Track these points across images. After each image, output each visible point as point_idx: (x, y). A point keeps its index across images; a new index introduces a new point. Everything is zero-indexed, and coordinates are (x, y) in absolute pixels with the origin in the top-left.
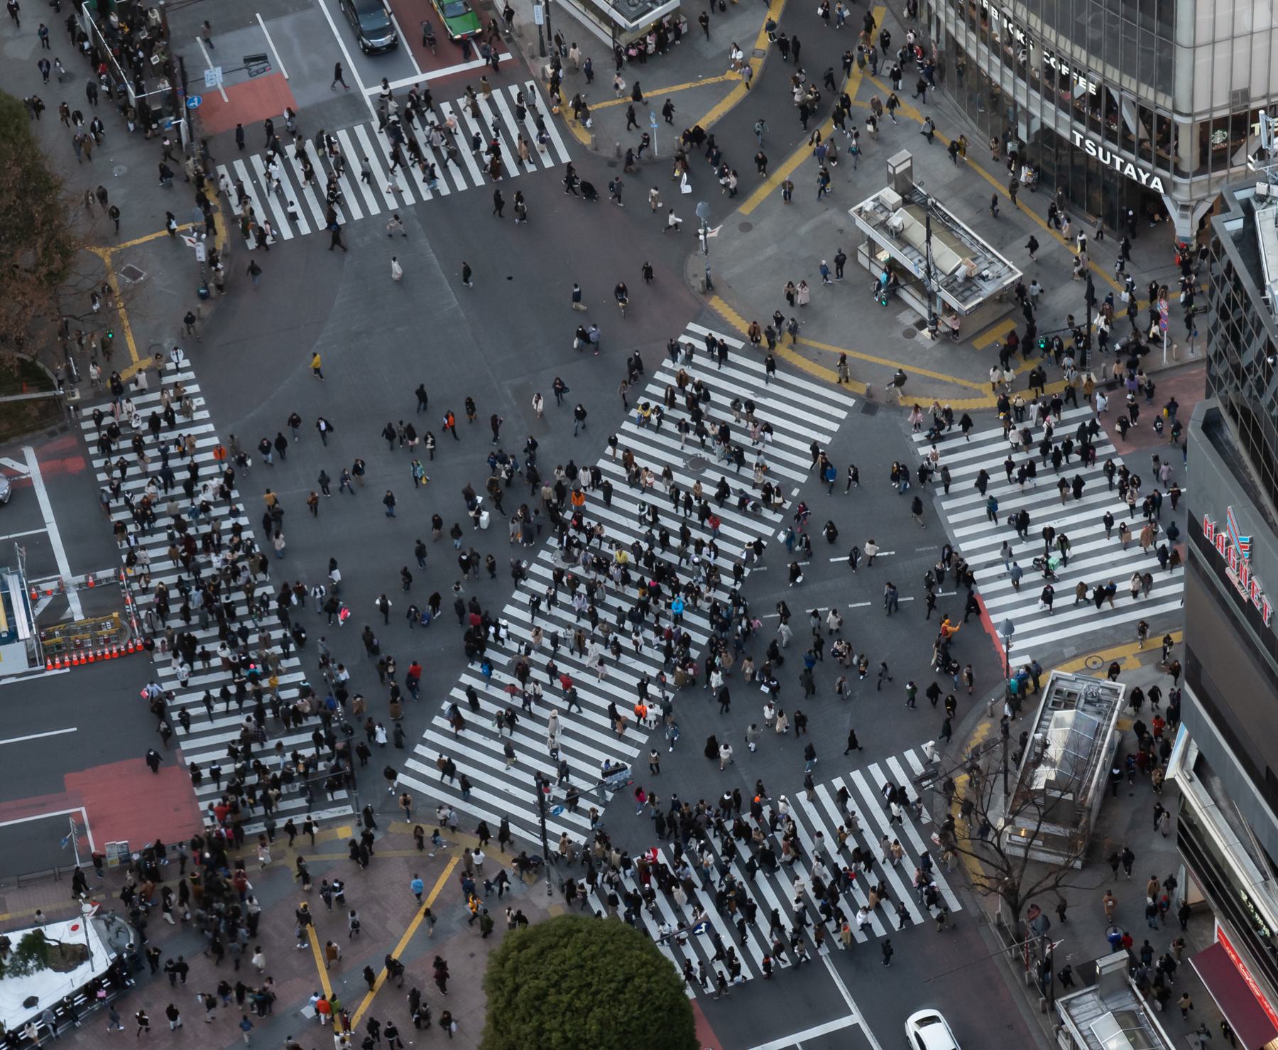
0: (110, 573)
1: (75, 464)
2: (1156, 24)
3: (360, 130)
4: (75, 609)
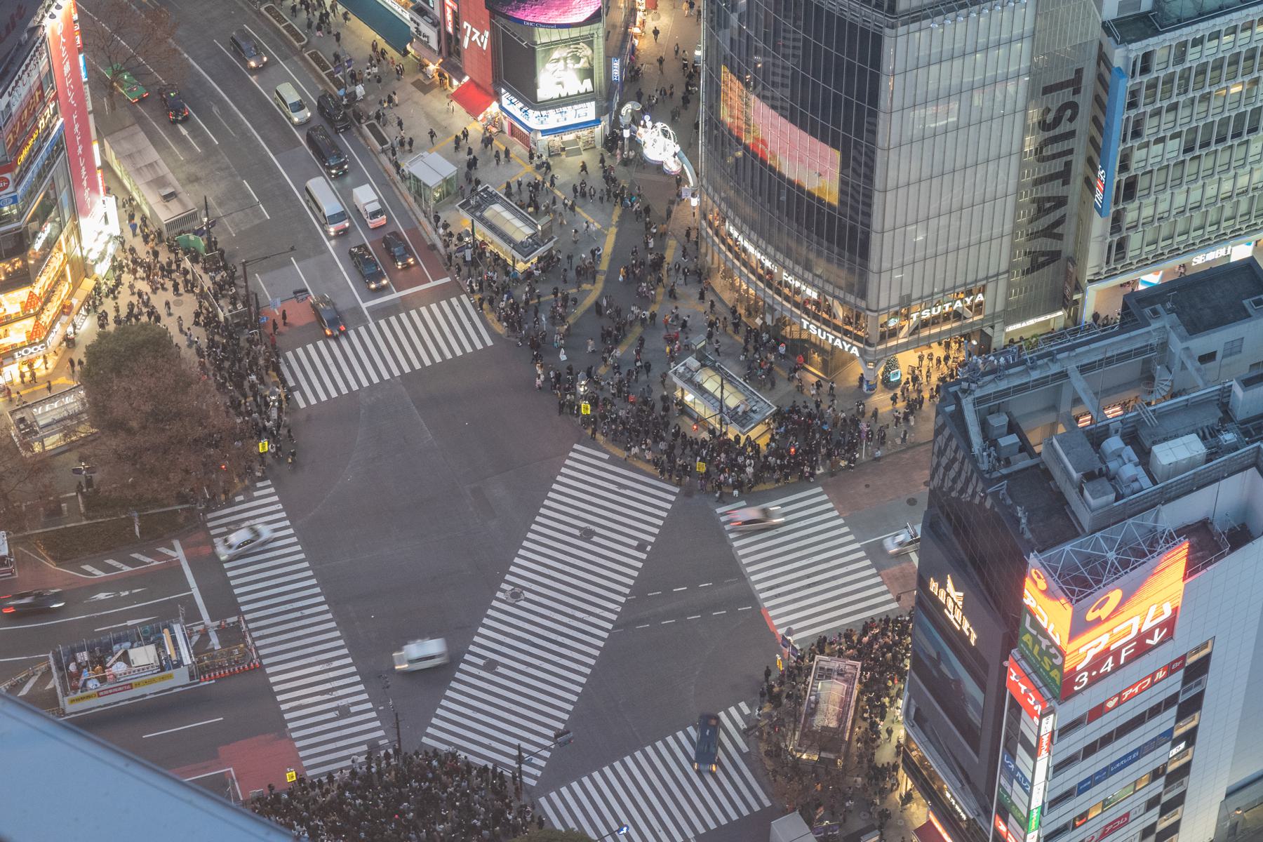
0: (235, 619)
1: (205, 550)
2: (858, 259)
3: (362, 330)
4: (215, 641)
